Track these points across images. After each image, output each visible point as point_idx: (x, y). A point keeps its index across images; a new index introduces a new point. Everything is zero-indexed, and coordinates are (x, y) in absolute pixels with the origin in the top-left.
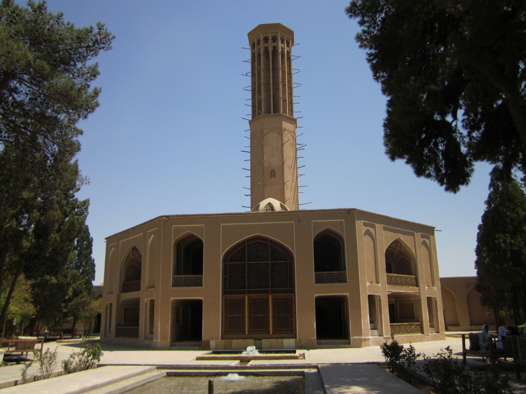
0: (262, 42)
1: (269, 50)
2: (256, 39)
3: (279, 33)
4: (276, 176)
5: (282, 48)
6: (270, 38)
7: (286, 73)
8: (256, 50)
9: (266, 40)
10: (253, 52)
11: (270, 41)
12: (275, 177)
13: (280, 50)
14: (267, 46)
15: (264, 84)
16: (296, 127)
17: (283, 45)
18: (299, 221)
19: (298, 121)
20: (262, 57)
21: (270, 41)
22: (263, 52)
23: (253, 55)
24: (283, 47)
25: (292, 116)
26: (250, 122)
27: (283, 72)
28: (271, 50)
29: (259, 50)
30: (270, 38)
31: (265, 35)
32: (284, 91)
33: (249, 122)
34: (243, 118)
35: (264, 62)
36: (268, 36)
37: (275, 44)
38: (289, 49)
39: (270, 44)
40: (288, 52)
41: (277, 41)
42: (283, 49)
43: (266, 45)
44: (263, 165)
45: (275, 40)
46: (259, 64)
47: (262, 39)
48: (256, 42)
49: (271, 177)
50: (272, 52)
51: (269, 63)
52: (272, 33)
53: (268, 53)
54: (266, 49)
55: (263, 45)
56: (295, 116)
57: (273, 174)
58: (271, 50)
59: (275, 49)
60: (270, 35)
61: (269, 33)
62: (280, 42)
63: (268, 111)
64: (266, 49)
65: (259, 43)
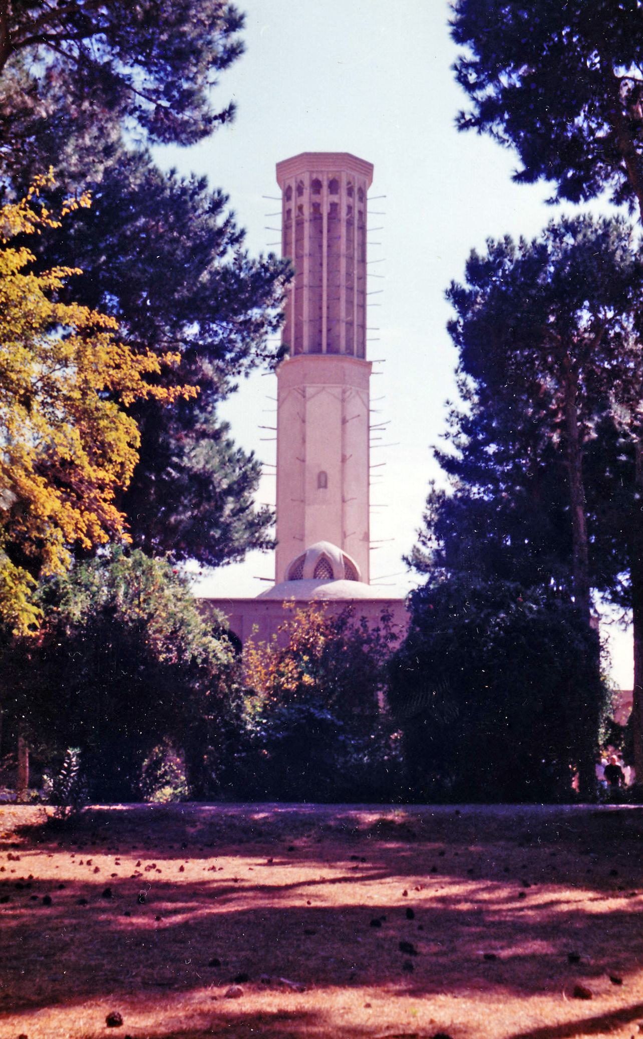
0: (307, 191)
2: (293, 180)
4: (329, 485)
5: (350, 208)
6: (325, 184)
7: (356, 262)
8: (292, 205)
9: (316, 185)
10: (287, 209)
11: (325, 190)
12: (325, 487)
13: (343, 214)
14: (318, 201)
15: (310, 287)
16: (370, 373)
17: (351, 200)
19: (375, 368)
20: (307, 225)
23: (287, 213)
25: (363, 355)
27: (350, 258)
28: (325, 210)
29: (300, 208)
30: (325, 184)
31: (314, 176)
32: (350, 302)
35: (310, 237)
37: (335, 198)
38: (362, 205)
39: (325, 199)
43: (317, 199)
44: (304, 461)
45: (334, 186)
46: (299, 240)
47: (307, 183)
48: (294, 188)
49: (320, 487)
50: (329, 214)
51: (321, 238)
52: (328, 172)
54: (316, 207)
56: (371, 355)
57: (322, 481)
58: (325, 210)
59: (334, 206)
60: (325, 178)
61: (322, 172)
62: (343, 191)
63: (316, 349)
64: (316, 207)
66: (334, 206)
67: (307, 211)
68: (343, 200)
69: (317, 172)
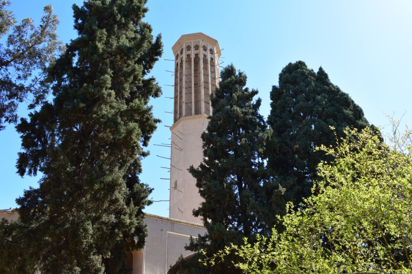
1: (191, 57)
3: (201, 42)
5: (205, 56)
6: (192, 47)
8: (179, 61)
9: (189, 48)
11: (193, 49)
13: (201, 57)
14: (190, 54)
18: (162, 230)
21: (193, 49)
22: (186, 59)
23: (177, 65)
24: (206, 54)
26: (171, 128)
28: (193, 57)
30: (192, 47)
31: (187, 45)
33: (170, 129)
34: (165, 125)
36: (190, 45)
39: (193, 52)
40: (212, 59)
41: (199, 48)
42: (205, 56)
45: (197, 47)
53: (191, 59)
54: (188, 56)
55: (186, 53)
59: (197, 55)
62: (201, 49)
63: (189, 113)
64: (188, 56)
65: (182, 53)
66: (197, 55)
67: (184, 59)
68: (201, 52)
69: (188, 43)
